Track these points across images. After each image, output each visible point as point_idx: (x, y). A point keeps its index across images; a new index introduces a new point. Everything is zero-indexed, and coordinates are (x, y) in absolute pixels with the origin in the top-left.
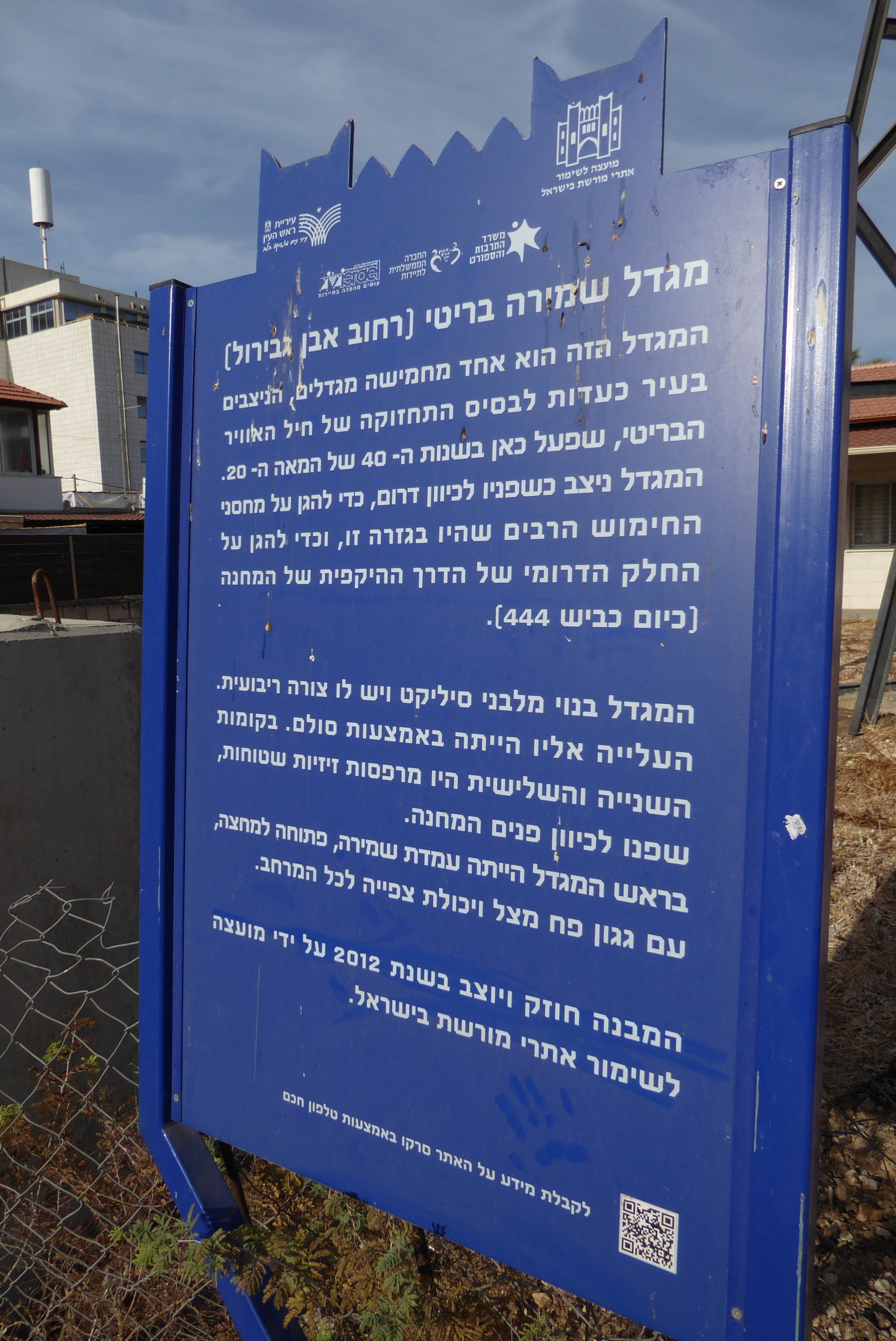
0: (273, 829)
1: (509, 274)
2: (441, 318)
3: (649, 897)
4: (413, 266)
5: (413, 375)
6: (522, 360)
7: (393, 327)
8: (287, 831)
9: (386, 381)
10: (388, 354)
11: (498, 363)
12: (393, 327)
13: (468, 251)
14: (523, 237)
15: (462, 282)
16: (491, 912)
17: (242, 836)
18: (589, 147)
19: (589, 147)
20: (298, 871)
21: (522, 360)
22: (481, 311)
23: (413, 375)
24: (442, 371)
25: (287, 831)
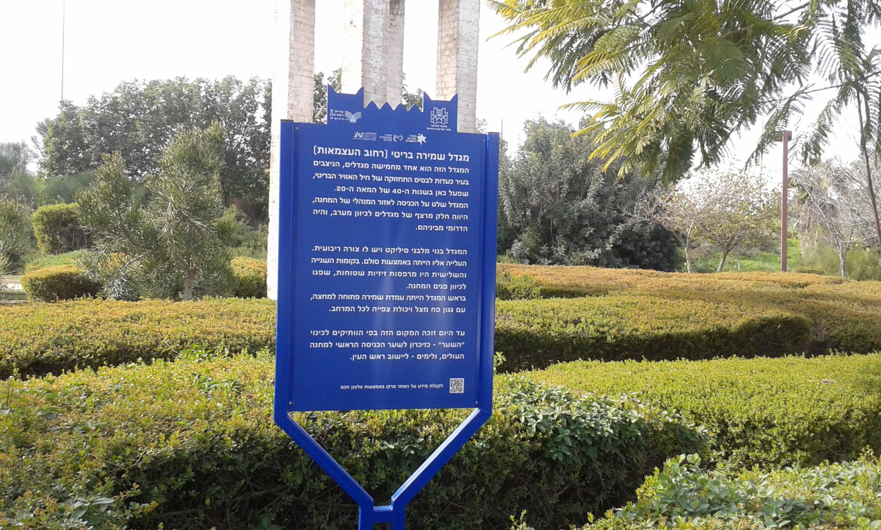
0: (337, 297)
1: (415, 148)
2: (397, 155)
3: (456, 298)
4: (388, 138)
5: (388, 167)
6: (422, 169)
7: (380, 154)
8: (342, 297)
9: (380, 167)
10: (379, 160)
11: (415, 168)
12: (380, 154)
13: (405, 138)
14: (421, 139)
15: (401, 146)
16: (414, 310)
17: (324, 300)
18: (439, 120)
19: (439, 120)
20: (347, 309)
21: (422, 169)
22: (409, 155)
23: (388, 167)
24: (398, 167)
25: (342, 297)
